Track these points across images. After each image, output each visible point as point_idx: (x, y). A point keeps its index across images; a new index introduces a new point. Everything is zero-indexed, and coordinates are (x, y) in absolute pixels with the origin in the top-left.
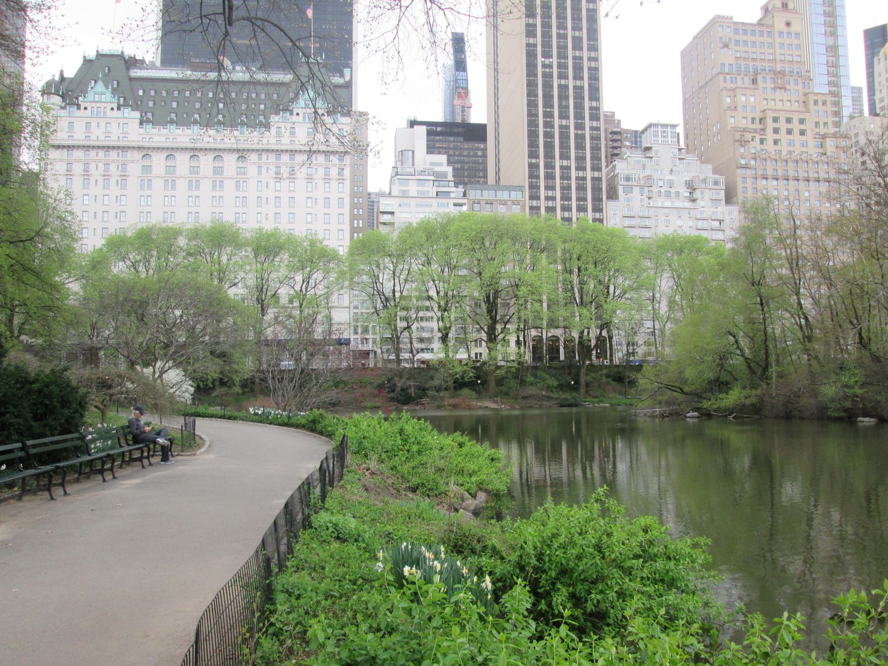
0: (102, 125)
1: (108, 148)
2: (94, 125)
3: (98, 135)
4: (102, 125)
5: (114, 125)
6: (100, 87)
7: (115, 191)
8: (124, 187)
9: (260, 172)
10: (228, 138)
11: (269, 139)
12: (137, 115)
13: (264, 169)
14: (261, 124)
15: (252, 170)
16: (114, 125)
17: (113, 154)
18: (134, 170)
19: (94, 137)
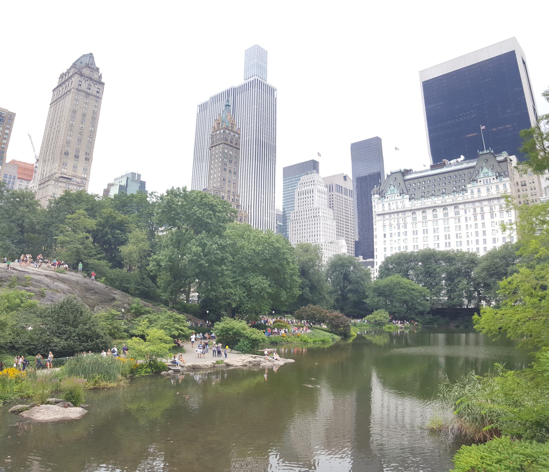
0: (394, 203)
1: (398, 212)
2: (391, 204)
3: (393, 207)
4: (394, 203)
5: (399, 202)
7: (402, 230)
8: (406, 228)
9: (466, 213)
10: (449, 199)
11: (468, 196)
12: (408, 196)
13: (468, 211)
14: (463, 190)
15: (462, 212)
16: (399, 202)
17: (400, 214)
18: (409, 220)
19: (392, 209)
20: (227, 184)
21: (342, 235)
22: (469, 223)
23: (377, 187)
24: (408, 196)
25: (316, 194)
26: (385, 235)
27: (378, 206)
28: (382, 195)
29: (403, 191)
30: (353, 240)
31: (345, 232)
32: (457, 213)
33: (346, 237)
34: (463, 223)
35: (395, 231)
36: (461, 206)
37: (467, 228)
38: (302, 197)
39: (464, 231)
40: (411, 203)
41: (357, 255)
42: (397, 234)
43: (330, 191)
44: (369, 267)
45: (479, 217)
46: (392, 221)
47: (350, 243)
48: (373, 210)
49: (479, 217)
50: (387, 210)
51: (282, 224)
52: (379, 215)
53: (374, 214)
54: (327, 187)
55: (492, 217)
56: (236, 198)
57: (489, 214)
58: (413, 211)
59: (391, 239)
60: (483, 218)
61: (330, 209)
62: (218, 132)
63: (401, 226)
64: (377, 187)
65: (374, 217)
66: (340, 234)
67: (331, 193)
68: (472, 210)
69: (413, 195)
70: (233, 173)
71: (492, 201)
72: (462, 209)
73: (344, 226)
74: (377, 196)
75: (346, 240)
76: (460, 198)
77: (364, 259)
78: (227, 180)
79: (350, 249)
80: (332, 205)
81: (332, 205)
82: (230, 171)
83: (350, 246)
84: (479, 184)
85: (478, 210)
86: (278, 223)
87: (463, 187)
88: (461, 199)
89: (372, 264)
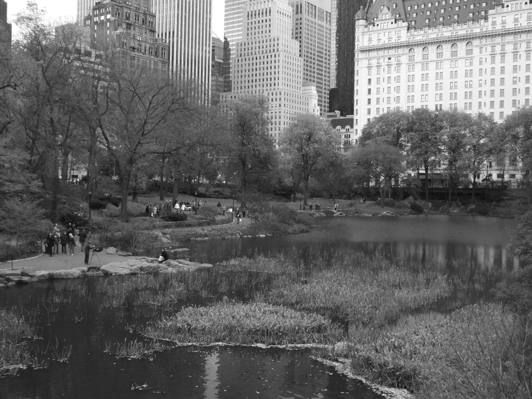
0: (387, 34)
3: (385, 40)
4: (387, 34)
6: (385, 10)
9: (481, 52)
10: (461, 30)
12: (406, 24)
13: (484, 49)
15: (476, 51)
18: (404, 59)
21: (312, 79)
22: (483, 67)
23: (364, 9)
24: (406, 24)
25: (275, 17)
26: (370, 80)
27: (363, 37)
28: (370, 21)
29: (400, 16)
30: (327, 88)
31: (316, 75)
32: (469, 52)
33: (317, 82)
34: (476, 67)
35: (384, 75)
36: (476, 42)
37: (480, 74)
38: (254, 20)
39: (476, 79)
40: (409, 34)
41: (331, 110)
42: (386, 80)
43: (297, 13)
44: (348, 127)
45: (498, 58)
46: (381, 60)
47: (323, 91)
48: (356, 44)
49: (498, 58)
50: (374, 43)
51: (221, 61)
52: (363, 51)
53: (356, 48)
54: (293, 6)
55: (515, 59)
56: (149, 19)
57: (512, 55)
58: (410, 46)
59: (378, 86)
60: (503, 60)
61: (294, 41)
63: (393, 68)
64: (364, 9)
65: (356, 53)
66: (309, 78)
67: (299, 16)
68: (489, 49)
69: (413, 23)
71: (519, 36)
72: (477, 46)
73: (316, 67)
74: (362, 22)
75: (317, 87)
76: (476, 28)
77: (342, 115)
79: (323, 99)
80: (299, 35)
81: (299, 35)
83: (323, 95)
84: (505, 9)
85: (498, 49)
86: (216, 60)
87: (483, 13)
88: (477, 30)
89: (351, 122)
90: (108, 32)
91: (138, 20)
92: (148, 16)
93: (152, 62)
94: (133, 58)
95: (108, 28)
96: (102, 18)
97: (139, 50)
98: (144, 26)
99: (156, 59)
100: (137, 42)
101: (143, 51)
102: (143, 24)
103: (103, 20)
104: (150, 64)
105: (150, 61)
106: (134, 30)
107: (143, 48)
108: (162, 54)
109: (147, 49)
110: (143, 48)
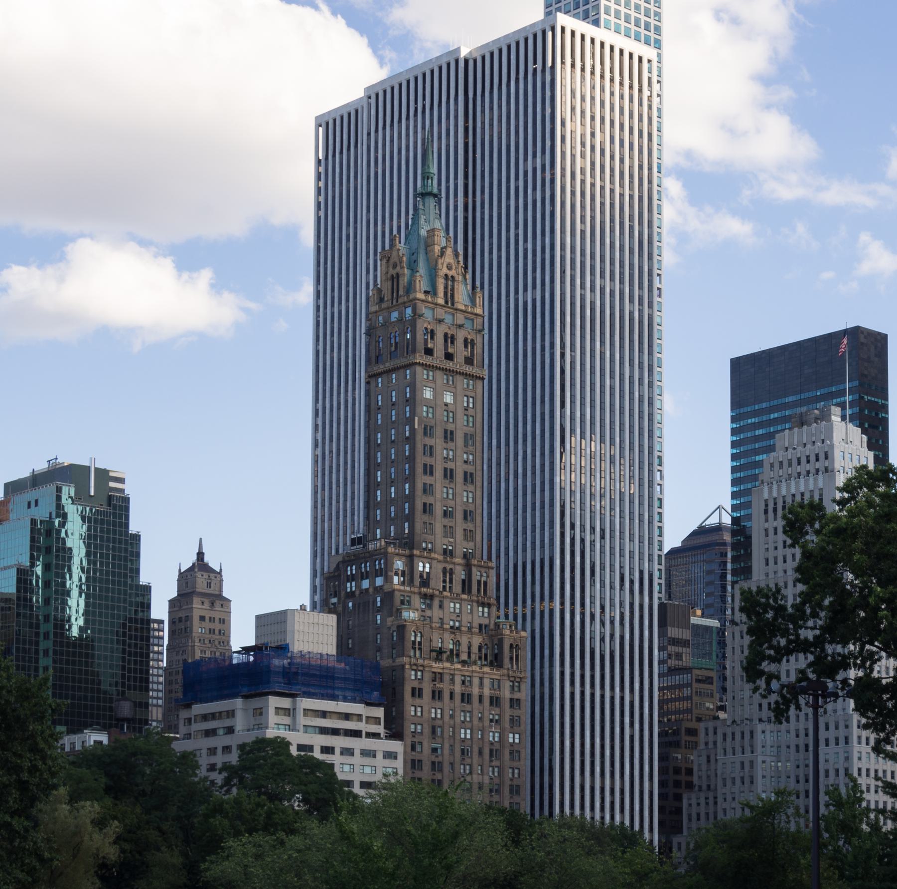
20: (439, 523)
62: (395, 315)
70: (459, 477)
78: (438, 510)
82: (449, 474)
90: (379, 617)
91: (451, 581)
92: (474, 569)
93: (487, 682)
94: (438, 677)
95: (379, 610)
96: (366, 584)
97: (453, 655)
98: (464, 596)
99: (496, 674)
100: (447, 636)
101: (464, 657)
102: (463, 592)
103: (367, 590)
104: (481, 684)
105: (481, 679)
106: (441, 607)
107: (464, 648)
108: (511, 658)
109: (475, 649)
110: (464, 648)
